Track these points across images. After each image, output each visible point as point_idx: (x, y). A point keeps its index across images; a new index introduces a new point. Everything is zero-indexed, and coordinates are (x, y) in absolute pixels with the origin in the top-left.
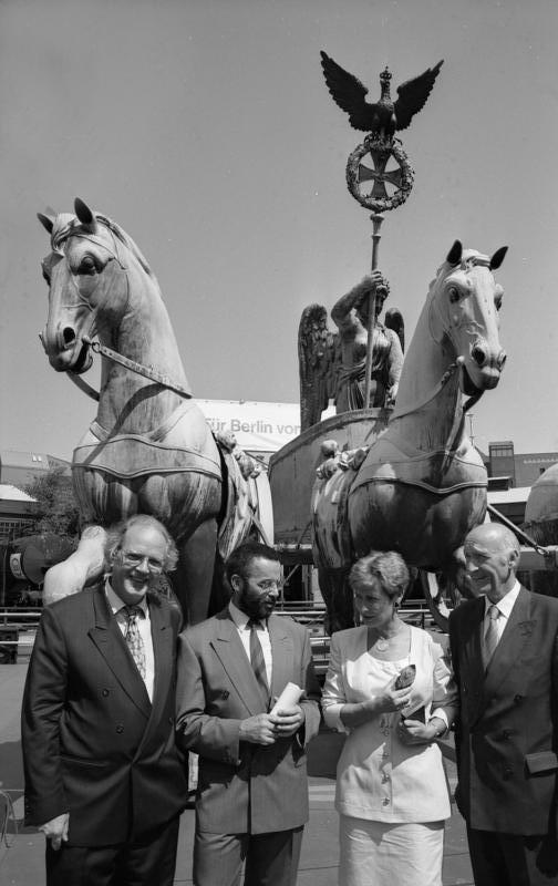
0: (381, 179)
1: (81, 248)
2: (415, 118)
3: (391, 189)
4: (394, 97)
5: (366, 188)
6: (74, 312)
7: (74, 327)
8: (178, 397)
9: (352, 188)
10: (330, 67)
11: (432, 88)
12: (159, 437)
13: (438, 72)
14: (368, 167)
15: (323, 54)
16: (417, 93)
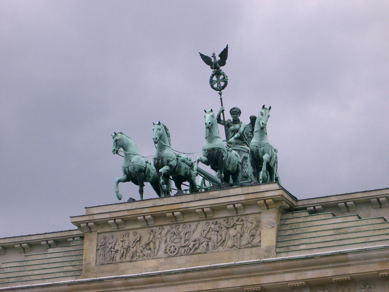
0: (219, 82)
1: (116, 138)
2: (226, 61)
3: (222, 84)
4: (218, 58)
5: (215, 86)
6: (115, 147)
7: (115, 149)
8: (134, 155)
9: (212, 87)
10: (202, 55)
11: (228, 52)
12: (130, 161)
13: (228, 48)
14: (220, 78)
15: (199, 53)
16: (224, 55)
